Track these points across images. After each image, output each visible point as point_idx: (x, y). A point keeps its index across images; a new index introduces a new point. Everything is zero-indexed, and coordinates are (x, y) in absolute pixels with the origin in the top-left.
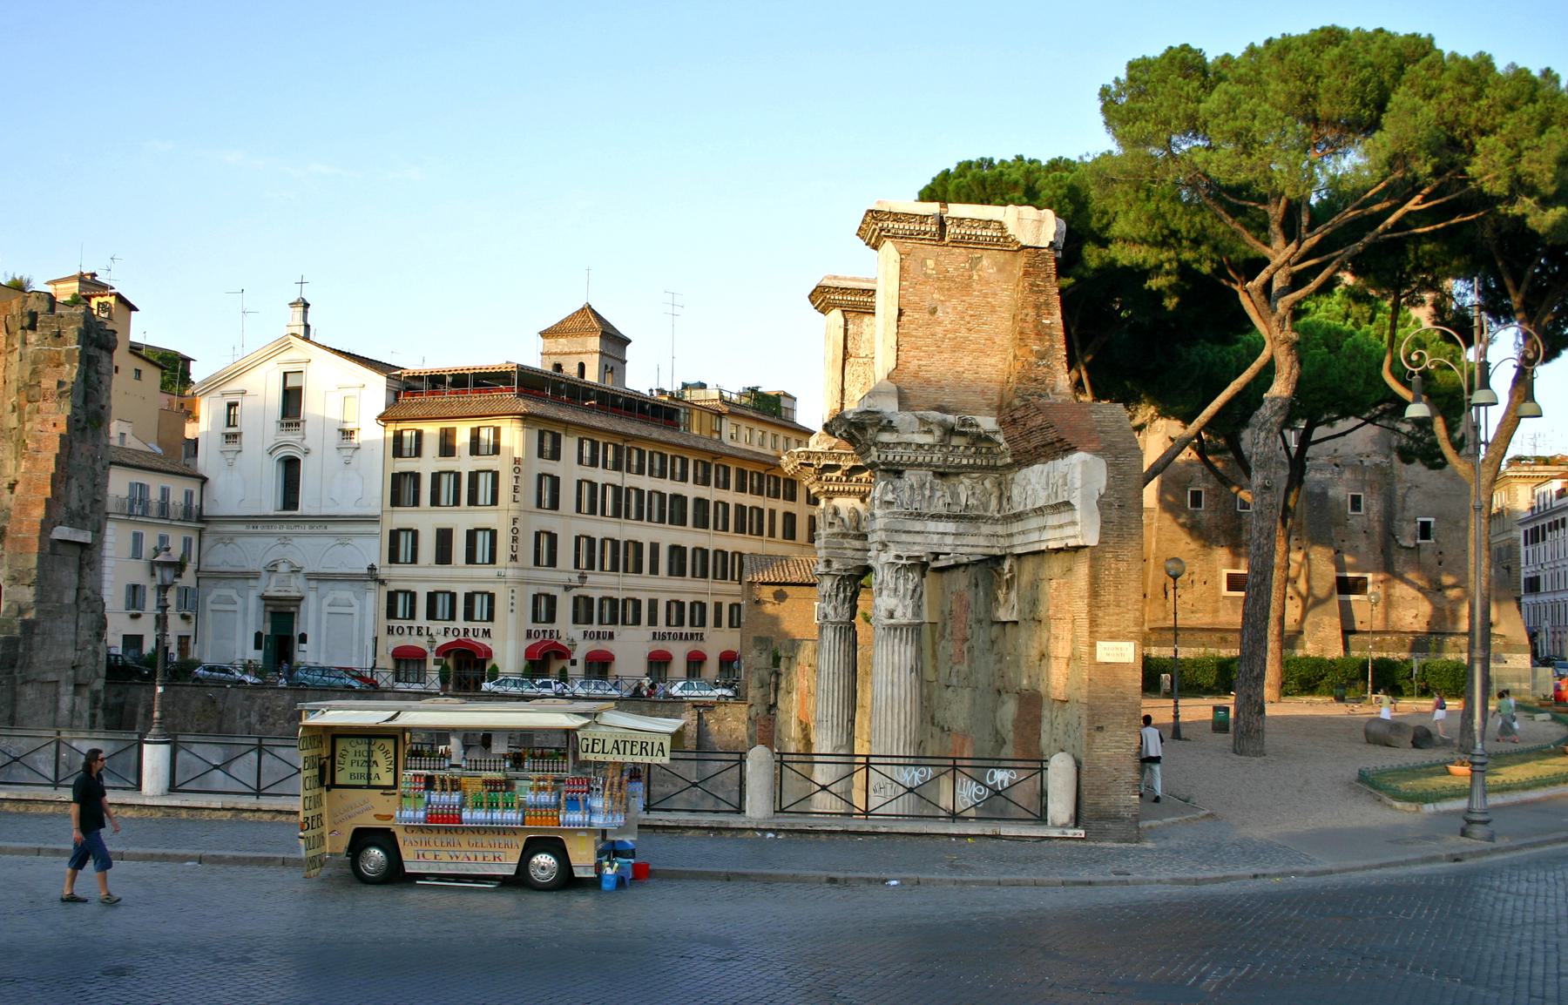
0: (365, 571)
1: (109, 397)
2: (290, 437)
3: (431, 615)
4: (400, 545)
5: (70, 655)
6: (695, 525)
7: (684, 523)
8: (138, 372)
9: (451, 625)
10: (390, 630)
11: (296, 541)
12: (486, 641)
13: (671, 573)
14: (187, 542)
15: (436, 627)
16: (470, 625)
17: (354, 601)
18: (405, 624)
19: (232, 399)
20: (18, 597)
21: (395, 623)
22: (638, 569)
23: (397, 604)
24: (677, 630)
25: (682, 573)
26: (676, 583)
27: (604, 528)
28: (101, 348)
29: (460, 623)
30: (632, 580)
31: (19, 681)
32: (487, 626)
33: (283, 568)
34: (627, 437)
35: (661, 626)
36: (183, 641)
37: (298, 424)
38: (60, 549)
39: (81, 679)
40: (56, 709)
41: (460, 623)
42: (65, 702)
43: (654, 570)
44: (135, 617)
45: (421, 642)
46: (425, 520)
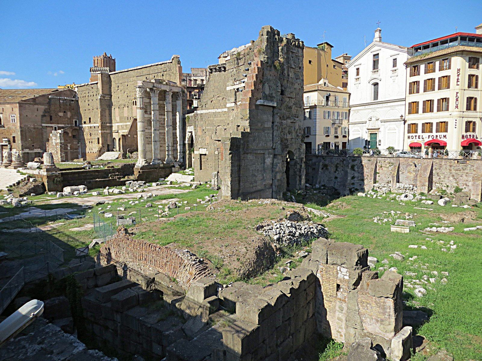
1: (302, 64)
2: (375, 76)
3: (423, 131)
4: (413, 108)
5: (270, 144)
8: (334, 66)
9: (431, 134)
10: (409, 137)
11: (377, 110)
12: (444, 140)
15: (426, 135)
16: (438, 134)
17: (396, 128)
18: (414, 135)
19: (357, 67)
20: (244, 124)
21: (410, 135)
23: (413, 128)
29: (434, 133)
31: (242, 153)
32: (445, 134)
33: (374, 119)
38: (261, 107)
39: (276, 153)
40: (264, 163)
41: (434, 133)
42: (268, 161)
44: (328, 136)
45: (420, 141)
46: (421, 97)
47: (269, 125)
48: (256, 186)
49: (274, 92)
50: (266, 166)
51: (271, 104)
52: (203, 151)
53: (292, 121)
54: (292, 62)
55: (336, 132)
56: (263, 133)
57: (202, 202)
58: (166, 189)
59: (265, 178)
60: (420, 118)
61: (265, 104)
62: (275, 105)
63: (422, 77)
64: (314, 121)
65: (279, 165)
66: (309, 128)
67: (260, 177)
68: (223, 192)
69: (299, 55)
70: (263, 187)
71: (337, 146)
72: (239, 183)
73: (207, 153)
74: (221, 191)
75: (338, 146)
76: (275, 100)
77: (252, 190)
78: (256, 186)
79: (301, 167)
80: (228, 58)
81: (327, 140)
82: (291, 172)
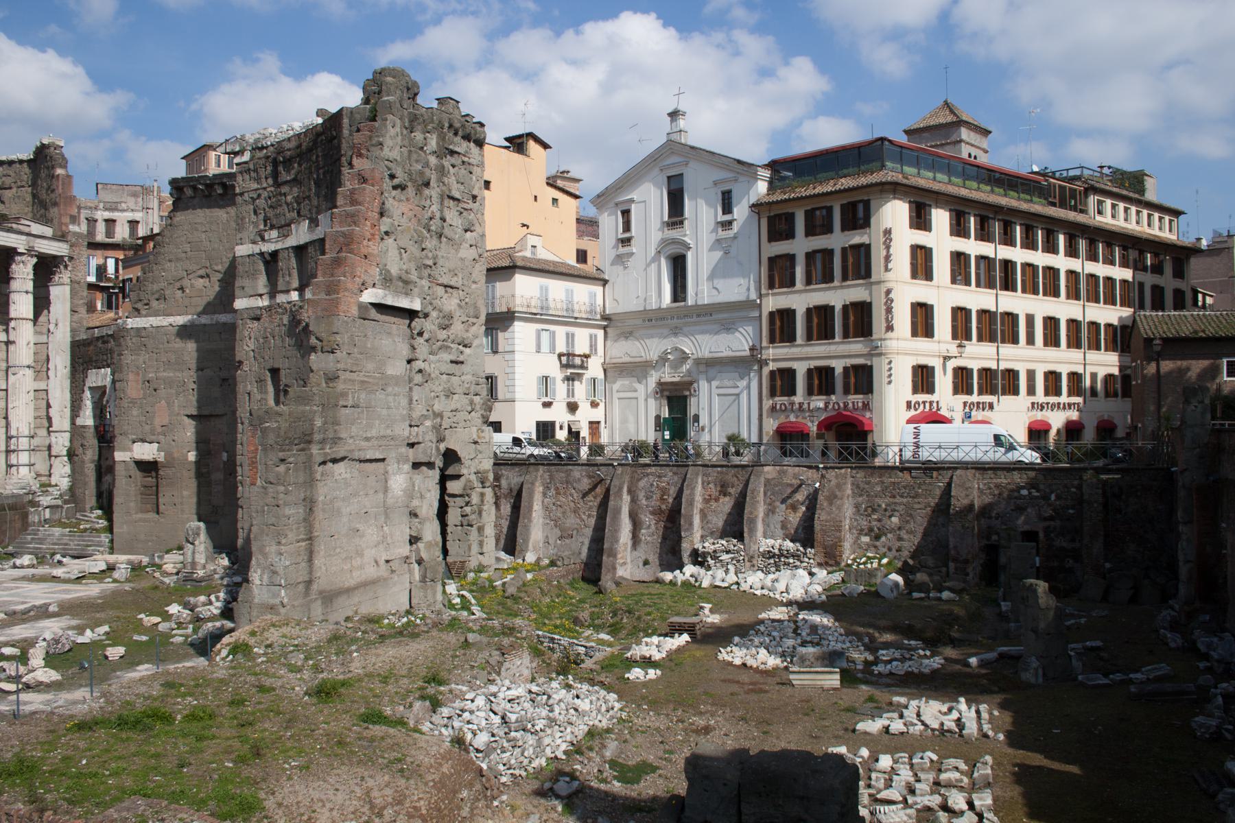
0: (748, 353)
2: (674, 234)
3: (810, 392)
6: (1068, 297)
7: (1056, 294)
8: (555, 201)
13: (1046, 344)
14: (593, 339)
15: (819, 402)
22: (1015, 340)
23: (783, 381)
24: (1053, 399)
25: (1057, 344)
26: (1051, 352)
27: (978, 299)
28: (467, 138)
30: (1007, 350)
34: (997, 209)
35: (1040, 396)
36: (594, 426)
37: (682, 223)
40: (386, 490)
43: (1031, 340)
44: (547, 405)
46: (800, 300)
47: (397, 368)
48: (361, 567)
49: (412, 266)
50: (390, 501)
51: (404, 303)
52: (146, 451)
53: (454, 358)
54: (451, 180)
55: (570, 393)
56: (380, 395)
57: (160, 628)
58: (19, 584)
59: (389, 540)
60: (802, 356)
61: (390, 301)
62: (416, 305)
63: (800, 245)
64: (507, 357)
65: (428, 495)
66: (491, 380)
67: (371, 533)
68: (256, 591)
69: (471, 161)
70: (383, 571)
71: (574, 435)
72: (310, 560)
73: (161, 457)
74: (250, 590)
75: (578, 433)
76: (416, 290)
77: (352, 583)
78: (361, 567)
79: (482, 501)
80: (246, 157)
81: (546, 416)
82: (453, 516)
